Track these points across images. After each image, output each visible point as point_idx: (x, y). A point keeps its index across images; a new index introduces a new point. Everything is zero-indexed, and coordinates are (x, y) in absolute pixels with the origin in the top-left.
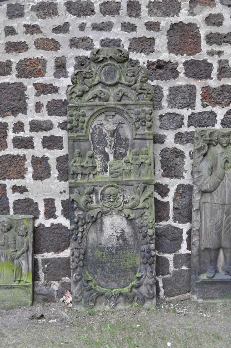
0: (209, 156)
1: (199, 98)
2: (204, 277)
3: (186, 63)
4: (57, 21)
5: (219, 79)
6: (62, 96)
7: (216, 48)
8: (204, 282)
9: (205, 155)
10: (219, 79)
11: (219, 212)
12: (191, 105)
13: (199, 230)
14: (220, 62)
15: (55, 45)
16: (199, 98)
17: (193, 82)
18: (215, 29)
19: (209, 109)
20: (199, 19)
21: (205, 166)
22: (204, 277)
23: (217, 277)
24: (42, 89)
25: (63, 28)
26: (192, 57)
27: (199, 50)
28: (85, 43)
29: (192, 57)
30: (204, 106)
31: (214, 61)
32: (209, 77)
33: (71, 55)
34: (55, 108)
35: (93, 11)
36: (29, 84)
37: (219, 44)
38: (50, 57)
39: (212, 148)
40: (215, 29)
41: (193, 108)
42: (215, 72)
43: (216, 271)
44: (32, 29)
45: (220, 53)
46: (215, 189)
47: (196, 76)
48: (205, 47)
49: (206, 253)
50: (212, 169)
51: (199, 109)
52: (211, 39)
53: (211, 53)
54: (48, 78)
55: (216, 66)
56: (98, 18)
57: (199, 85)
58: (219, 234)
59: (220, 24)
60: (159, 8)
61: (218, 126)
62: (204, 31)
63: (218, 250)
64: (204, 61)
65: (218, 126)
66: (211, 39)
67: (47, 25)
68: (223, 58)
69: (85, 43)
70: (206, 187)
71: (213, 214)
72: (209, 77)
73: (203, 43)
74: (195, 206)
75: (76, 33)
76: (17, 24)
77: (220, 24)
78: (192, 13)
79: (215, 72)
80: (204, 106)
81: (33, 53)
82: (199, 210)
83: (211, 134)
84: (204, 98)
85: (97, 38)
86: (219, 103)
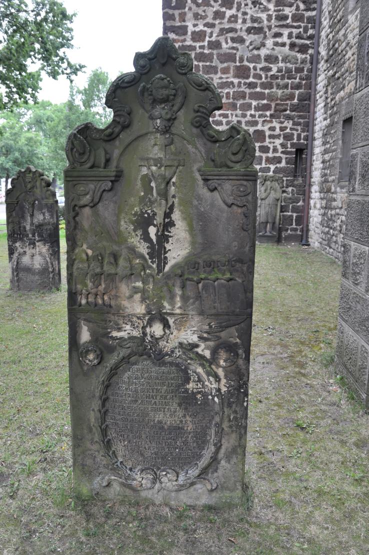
0: (265, 185)
1: (264, 161)
2: (261, 234)
3: (259, 147)
5: (273, 153)
7: (272, 140)
8: (260, 236)
9: (263, 185)
10: (273, 153)
11: (267, 208)
12: (260, 164)
13: (260, 215)
14: (273, 146)
16: (264, 161)
17: (262, 154)
18: (272, 133)
19: (268, 166)
20: (266, 128)
21: (263, 189)
22: (261, 234)
23: (266, 234)
26: (262, 144)
27: (264, 141)
29: (262, 144)
30: (266, 164)
31: (271, 146)
32: (268, 152)
35: (222, 124)
37: (274, 139)
39: (267, 182)
40: (272, 133)
41: (261, 165)
42: (271, 151)
43: (266, 232)
45: (274, 143)
46: (266, 198)
47: (263, 152)
48: (267, 140)
49: (261, 225)
50: (266, 190)
51: (263, 165)
52: (271, 137)
53: (270, 143)
55: (272, 148)
57: (264, 156)
58: (267, 216)
59: (274, 130)
60: (250, 123)
61: (271, 173)
62: (267, 133)
63: (267, 223)
64: (267, 146)
65: (271, 173)
66: (271, 137)
68: (275, 145)
70: (263, 197)
71: (265, 208)
72: (268, 152)
73: (267, 138)
74: (259, 205)
77: (274, 130)
78: (263, 126)
79: (271, 151)
80: (266, 164)
82: (260, 206)
83: (266, 176)
84: (266, 161)
86: (272, 164)
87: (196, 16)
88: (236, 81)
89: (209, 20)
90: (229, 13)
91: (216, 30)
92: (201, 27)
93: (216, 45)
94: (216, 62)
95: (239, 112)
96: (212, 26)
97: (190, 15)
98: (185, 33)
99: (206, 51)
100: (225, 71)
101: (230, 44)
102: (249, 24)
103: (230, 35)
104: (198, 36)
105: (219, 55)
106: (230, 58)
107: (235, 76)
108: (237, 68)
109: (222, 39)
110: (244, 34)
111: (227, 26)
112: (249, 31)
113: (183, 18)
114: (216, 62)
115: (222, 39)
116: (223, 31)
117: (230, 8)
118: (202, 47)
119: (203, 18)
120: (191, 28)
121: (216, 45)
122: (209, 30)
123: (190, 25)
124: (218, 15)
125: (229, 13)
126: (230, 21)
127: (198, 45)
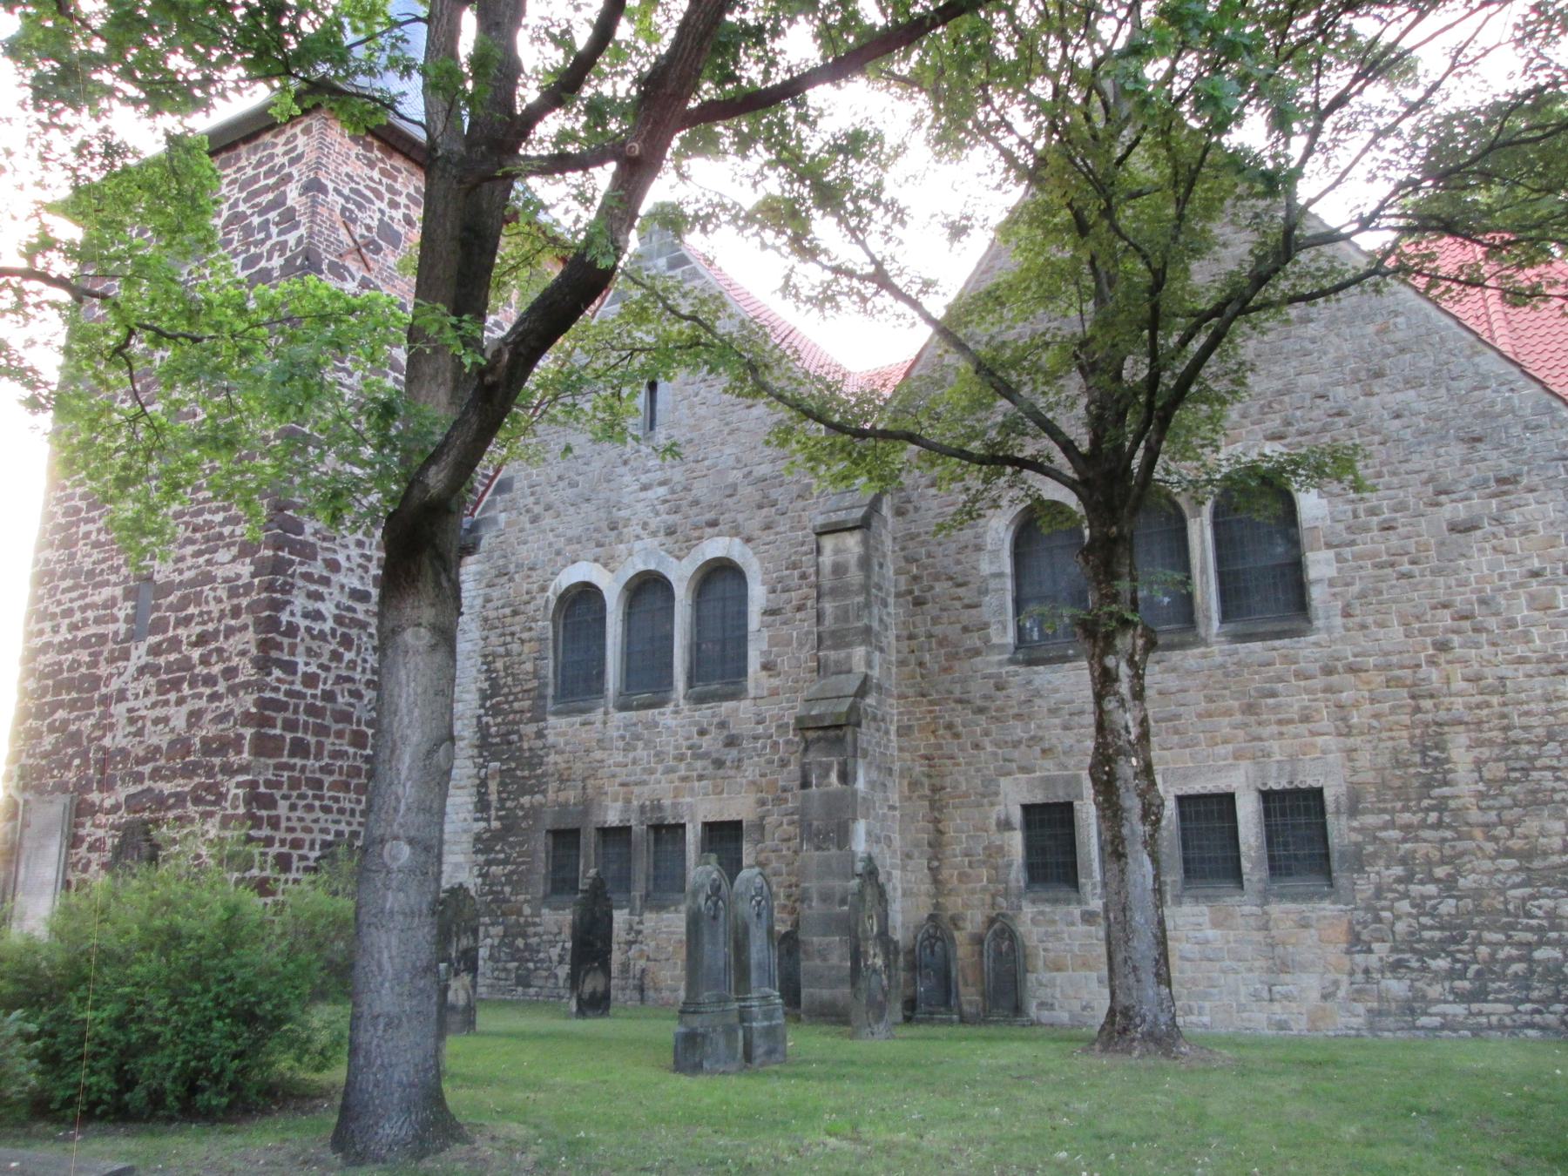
4: (313, 816)
6: (312, 863)
15: (310, 830)
24: (303, 858)
25: (316, 821)
28: (324, 831)
33: (319, 837)
34: (307, 869)
36: (295, 854)
38: (307, 837)
44: (301, 819)
54: (305, 851)
56: (335, 816)
67: (309, 817)
69: (324, 831)
75: (322, 824)
76: (294, 815)
81: (299, 835)
85: (333, 828)
87: (309, 651)
88: (351, 750)
89: (325, 660)
90: (349, 656)
91: (332, 676)
92: (313, 669)
93: (329, 696)
94: (328, 721)
95: (353, 796)
96: (326, 669)
97: (301, 649)
98: (295, 673)
99: (319, 703)
100: (340, 734)
101: (347, 699)
102: (368, 676)
103: (347, 686)
104: (310, 680)
105: (333, 711)
106: (344, 717)
107: (352, 744)
108: (355, 733)
109: (337, 689)
110: (362, 687)
111: (344, 673)
112: (369, 683)
113: (293, 647)
114: (328, 721)
115: (337, 689)
116: (340, 679)
117: (349, 649)
118: (314, 696)
119: (318, 655)
120: (301, 668)
121: (329, 696)
122: (323, 675)
123: (300, 660)
124: (336, 656)
125: (349, 656)
126: (348, 668)
127: (309, 692)
